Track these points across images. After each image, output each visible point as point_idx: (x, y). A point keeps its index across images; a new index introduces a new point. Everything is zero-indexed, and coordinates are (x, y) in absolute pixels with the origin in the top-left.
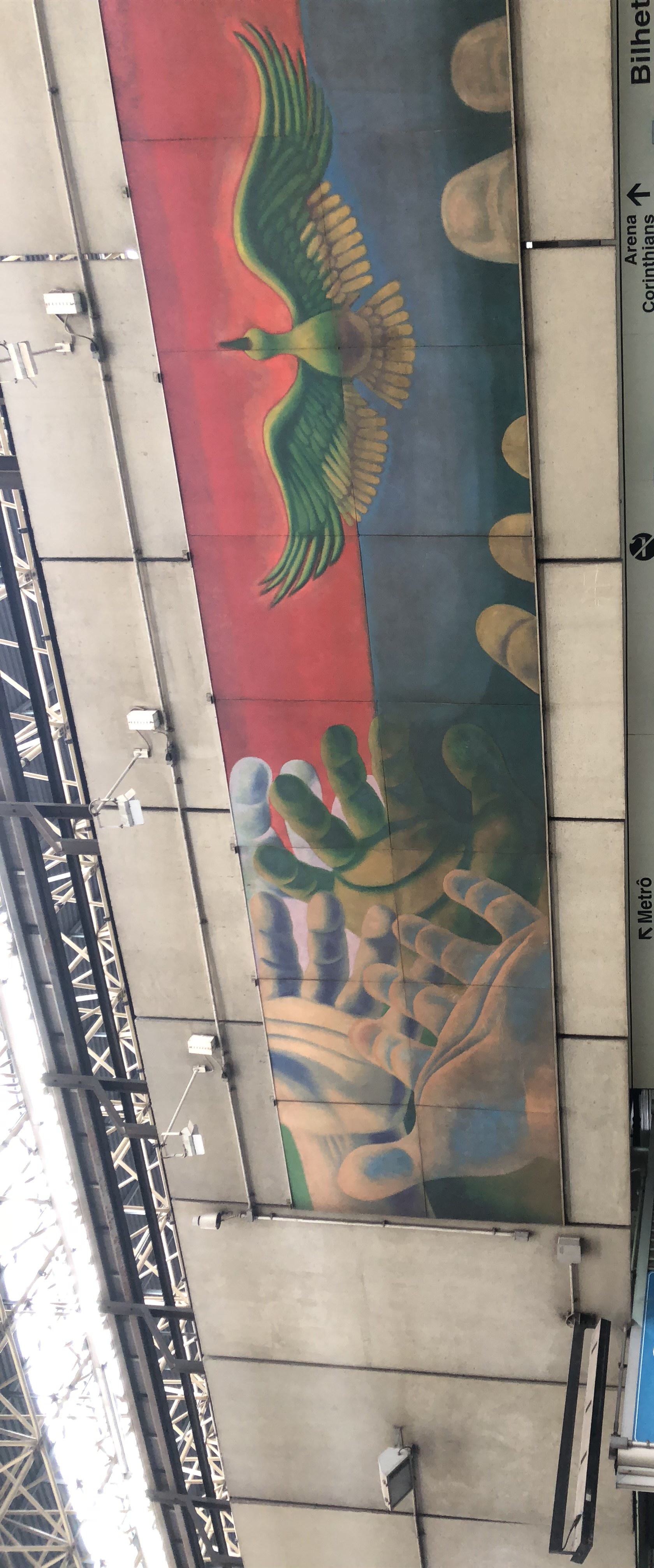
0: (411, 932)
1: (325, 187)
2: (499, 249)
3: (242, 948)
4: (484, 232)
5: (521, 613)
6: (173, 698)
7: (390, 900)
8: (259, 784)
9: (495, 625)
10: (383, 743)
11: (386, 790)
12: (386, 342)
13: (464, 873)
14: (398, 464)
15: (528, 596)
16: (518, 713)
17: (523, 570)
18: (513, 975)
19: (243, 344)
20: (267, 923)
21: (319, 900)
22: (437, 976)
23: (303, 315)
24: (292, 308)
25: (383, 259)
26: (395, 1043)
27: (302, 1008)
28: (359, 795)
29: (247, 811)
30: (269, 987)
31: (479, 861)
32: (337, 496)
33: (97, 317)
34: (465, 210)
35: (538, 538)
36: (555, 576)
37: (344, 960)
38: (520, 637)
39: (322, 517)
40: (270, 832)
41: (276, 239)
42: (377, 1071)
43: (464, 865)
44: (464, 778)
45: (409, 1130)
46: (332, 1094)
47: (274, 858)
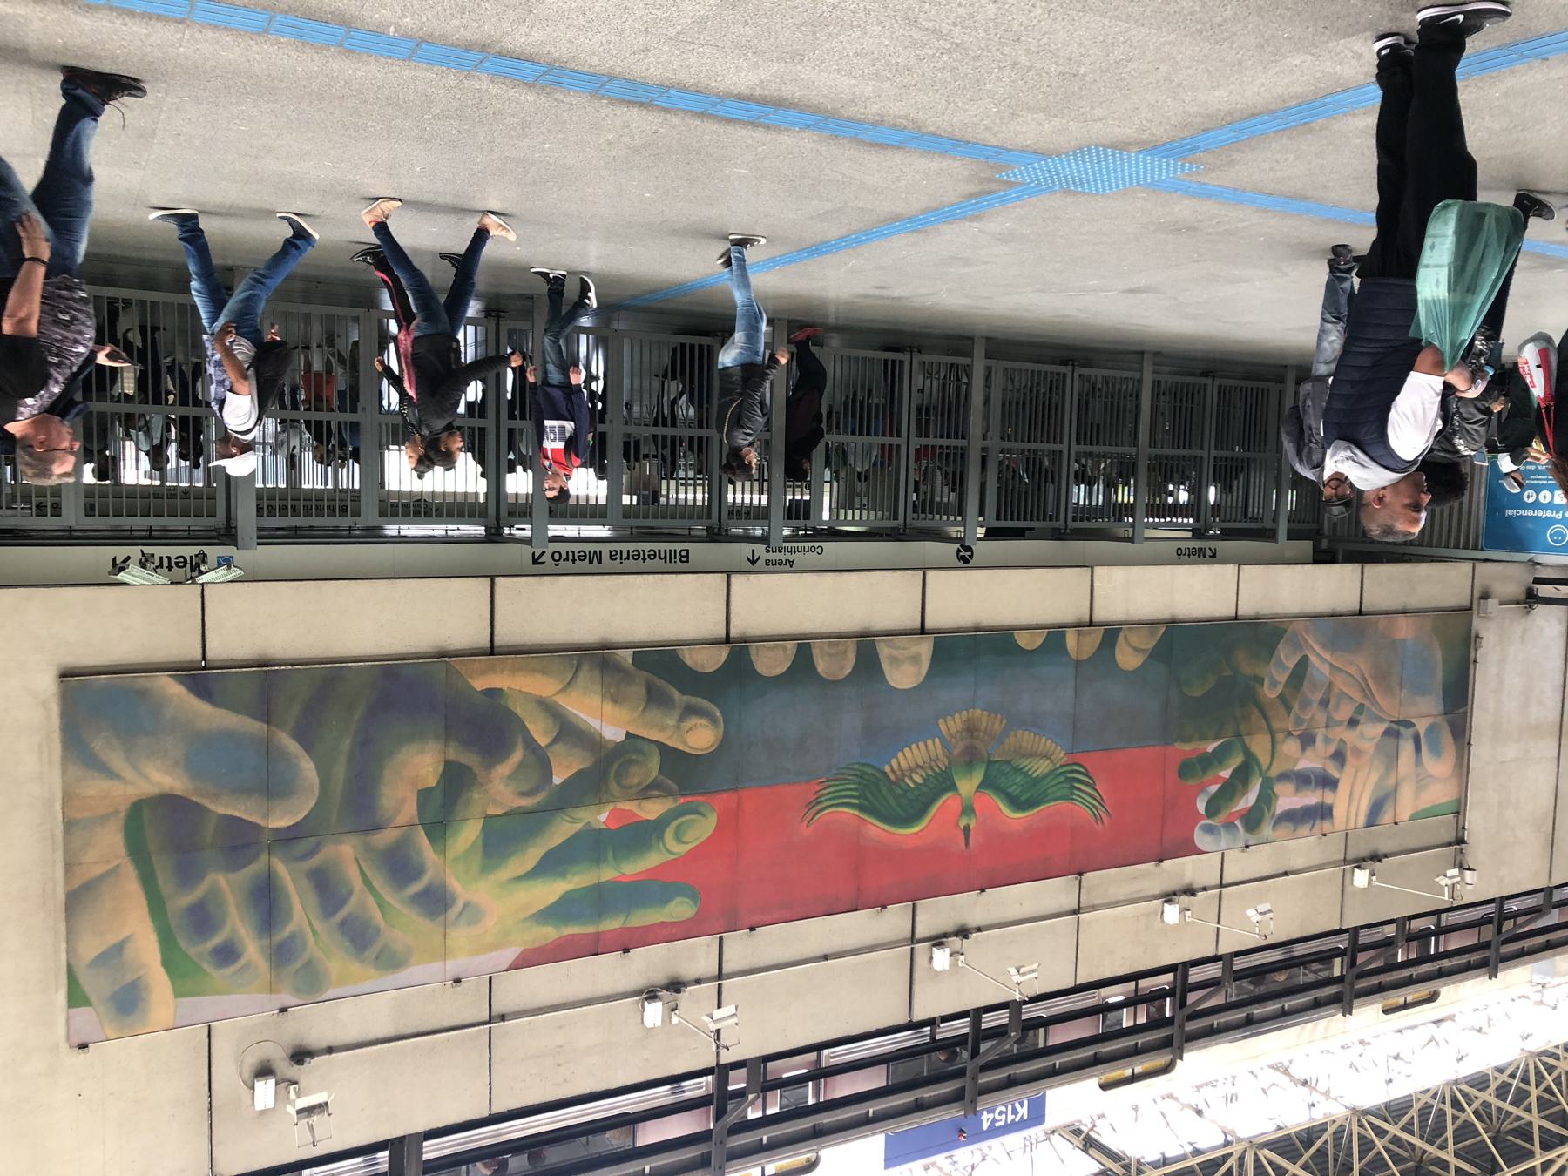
0: (1299, 721)
1: (887, 769)
2: (925, 648)
3: (1302, 847)
4: (915, 659)
6: (1157, 891)
7: (1280, 736)
8: (1209, 830)
11: (1216, 738)
12: (971, 729)
14: (1034, 723)
15: (1112, 632)
16: (1181, 640)
18: (1324, 646)
19: (967, 829)
20: (1290, 826)
21: (1279, 788)
22: (1325, 703)
23: (953, 787)
24: (950, 794)
25: (926, 730)
26: (1362, 734)
27: (1339, 801)
28: (1219, 757)
29: (1225, 839)
30: (1326, 826)
31: (1258, 672)
32: (1051, 767)
33: (945, 935)
34: (905, 671)
35: (1078, 625)
37: (1312, 770)
39: (1062, 779)
40: (1238, 823)
41: (912, 807)
42: (1378, 747)
44: (1211, 681)
45: (1413, 725)
46: (1391, 782)
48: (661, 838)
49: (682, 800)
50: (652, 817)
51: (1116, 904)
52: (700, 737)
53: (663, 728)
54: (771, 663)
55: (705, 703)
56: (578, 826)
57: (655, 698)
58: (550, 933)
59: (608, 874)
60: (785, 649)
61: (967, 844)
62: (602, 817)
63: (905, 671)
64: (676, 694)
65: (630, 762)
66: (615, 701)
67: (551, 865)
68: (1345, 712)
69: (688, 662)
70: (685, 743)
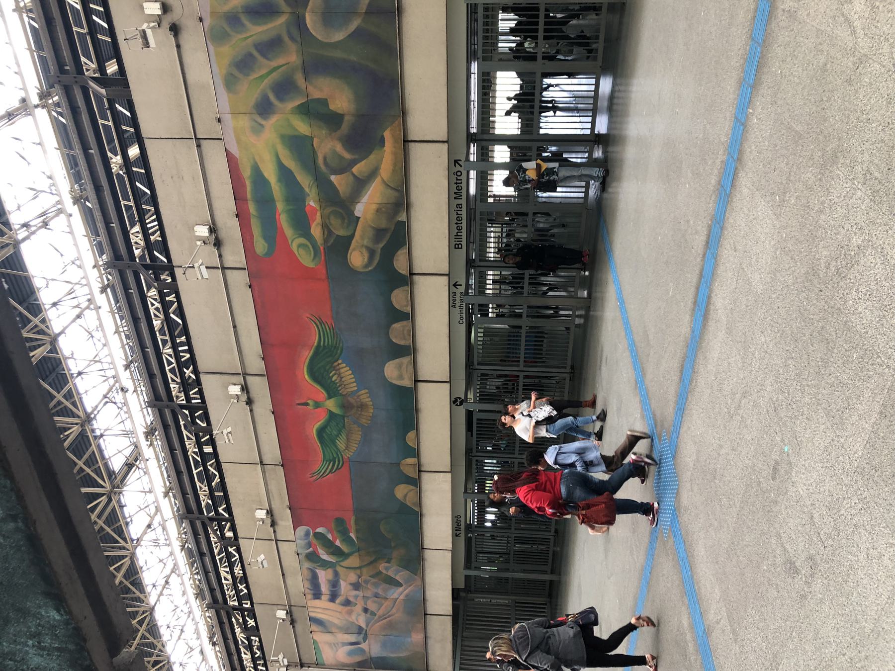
1: (340, 361)
2: (407, 382)
4: (401, 377)
5: (412, 487)
7: (358, 572)
8: (307, 534)
9: (401, 491)
10: (356, 523)
11: (357, 538)
12: (362, 406)
13: (387, 565)
15: (416, 482)
16: (411, 520)
17: (413, 474)
19: (307, 404)
20: (309, 577)
23: (330, 397)
28: (347, 540)
30: (309, 596)
32: (341, 450)
33: (248, 392)
34: (394, 371)
36: (425, 477)
38: (411, 494)
41: (319, 374)
43: (388, 562)
46: (334, 630)
47: (312, 557)
48: (301, 236)
49: (322, 248)
50: (312, 231)
51: (266, 484)
52: (357, 258)
53: (362, 238)
54: (399, 298)
55: (376, 262)
56: (307, 190)
57: (379, 233)
58: (246, 173)
59: (280, 206)
60: (407, 306)
61: (299, 404)
62: (312, 203)
63: (394, 371)
64: (381, 245)
65: (343, 219)
66: (378, 211)
67: (285, 174)
68: (372, 606)
69: (399, 252)
70: (354, 250)
